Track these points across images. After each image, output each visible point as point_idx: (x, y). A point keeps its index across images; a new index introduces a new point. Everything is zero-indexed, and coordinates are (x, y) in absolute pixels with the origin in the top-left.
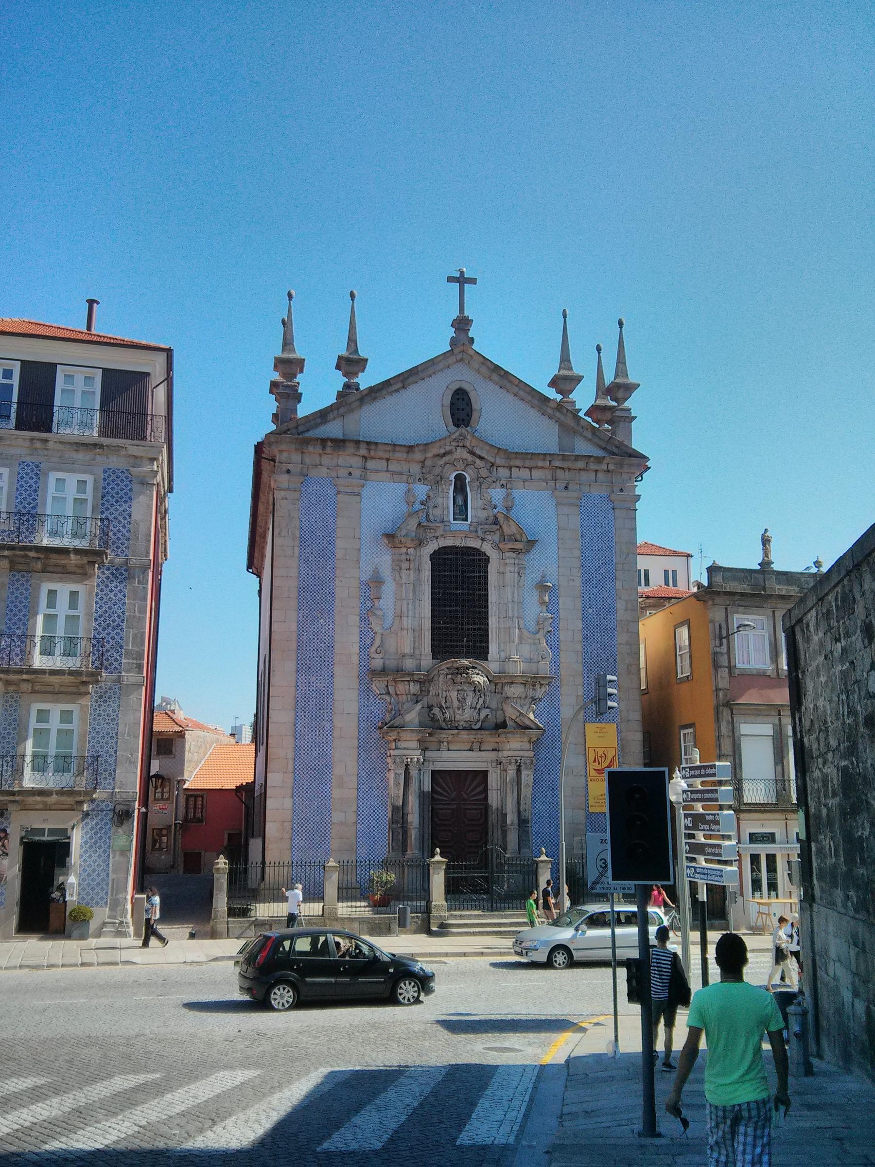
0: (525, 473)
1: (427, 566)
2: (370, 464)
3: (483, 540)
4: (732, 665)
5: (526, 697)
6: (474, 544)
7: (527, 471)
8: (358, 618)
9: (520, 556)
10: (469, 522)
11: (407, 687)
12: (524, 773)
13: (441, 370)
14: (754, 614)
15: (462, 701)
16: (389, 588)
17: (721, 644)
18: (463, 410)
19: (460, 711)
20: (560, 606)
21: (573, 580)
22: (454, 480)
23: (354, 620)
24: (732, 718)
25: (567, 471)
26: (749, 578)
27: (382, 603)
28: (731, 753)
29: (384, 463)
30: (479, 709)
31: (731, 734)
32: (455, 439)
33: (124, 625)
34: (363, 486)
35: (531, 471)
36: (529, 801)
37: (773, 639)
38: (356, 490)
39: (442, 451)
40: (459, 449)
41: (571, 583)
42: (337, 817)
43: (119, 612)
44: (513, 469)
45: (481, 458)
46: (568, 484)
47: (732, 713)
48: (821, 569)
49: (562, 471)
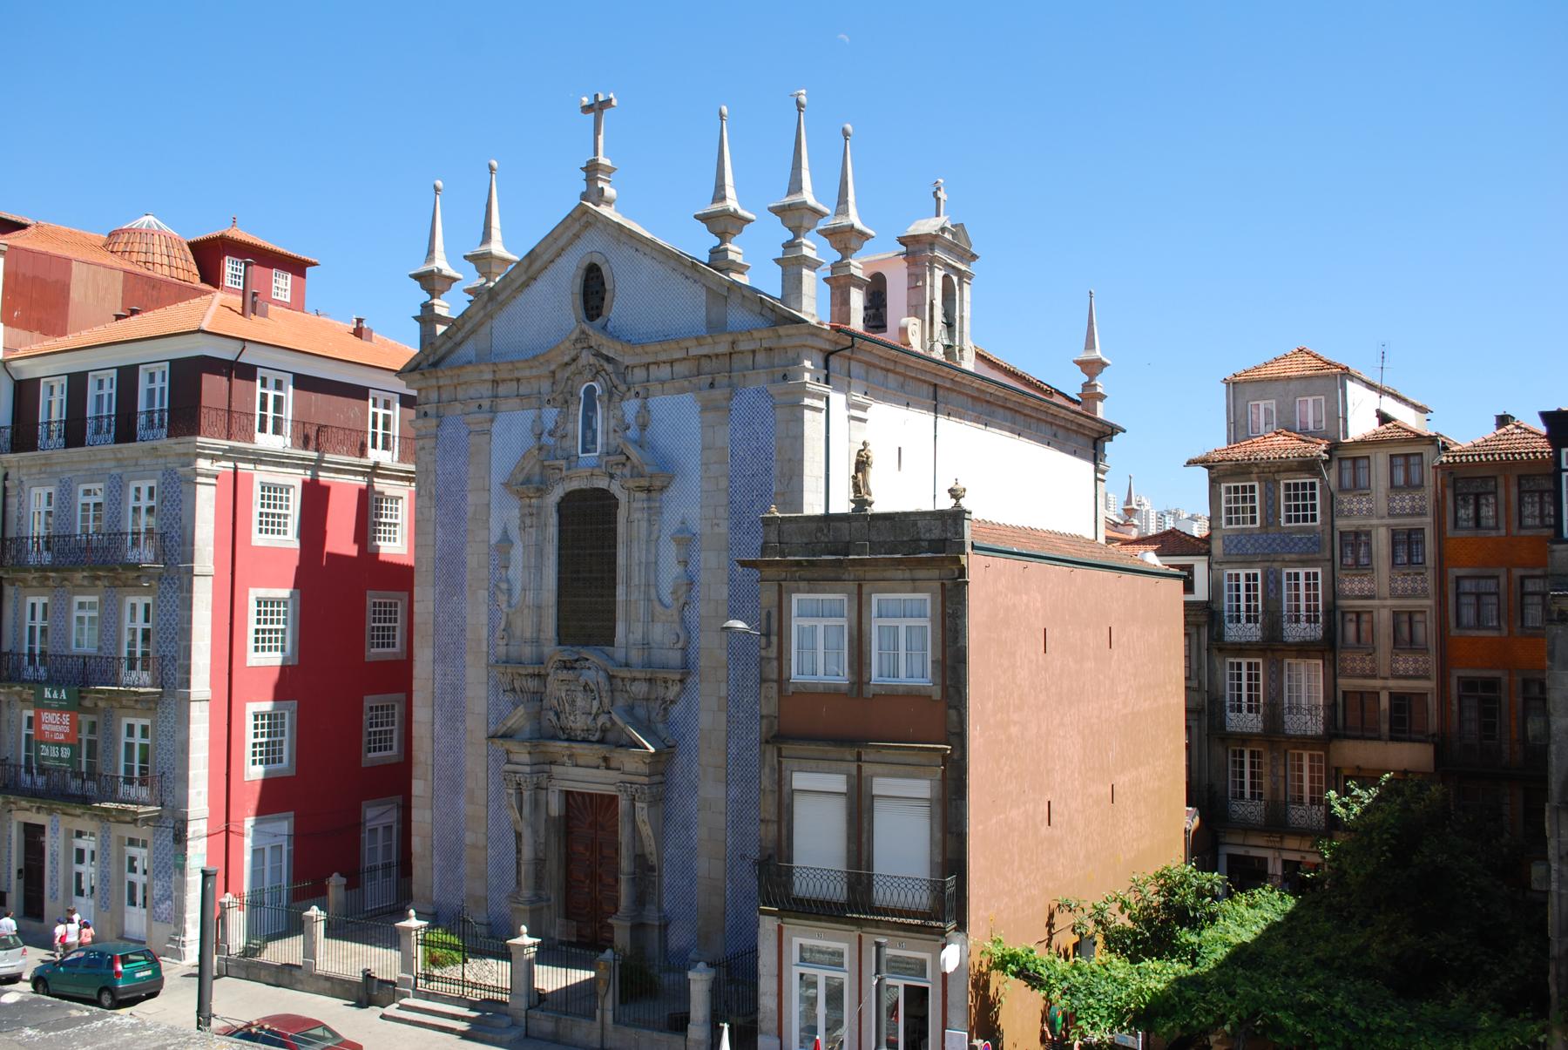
0: (665, 371)
1: (553, 520)
2: (502, 390)
3: (612, 476)
4: (784, 677)
5: (657, 698)
6: (602, 483)
7: (668, 368)
8: (486, 593)
9: (654, 494)
10: (597, 454)
11: (524, 683)
12: (638, 805)
13: (570, 243)
14: (824, 591)
15: (573, 703)
16: (517, 553)
17: (769, 644)
18: (597, 292)
19: (572, 718)
20: (702, 565)
21: (718, 525)
22: (582, 396)
23: (483, 594)
24: (780, 763)
25: (714, 359)
26: (825, 531)
27: (511, 572)
28: (774, 818)
29: (515, 384)
30: (597, 715)
31: (776, 787)
32: (577, 340)
33: (177, 638)
34: (492, 421)
35: (672, 366)
36: (653, 843)
37: (855, 633)
38: (486, 426)
39: (567, 359)
40: (584, 353)
41: (716, 530)
42: (469, 838)
43: (174, 623)
44: (651, 367)
45: (608, 359)
46: (714, 379)
47: (780, 755)
48: (961, 501)
49: (708, 361)
